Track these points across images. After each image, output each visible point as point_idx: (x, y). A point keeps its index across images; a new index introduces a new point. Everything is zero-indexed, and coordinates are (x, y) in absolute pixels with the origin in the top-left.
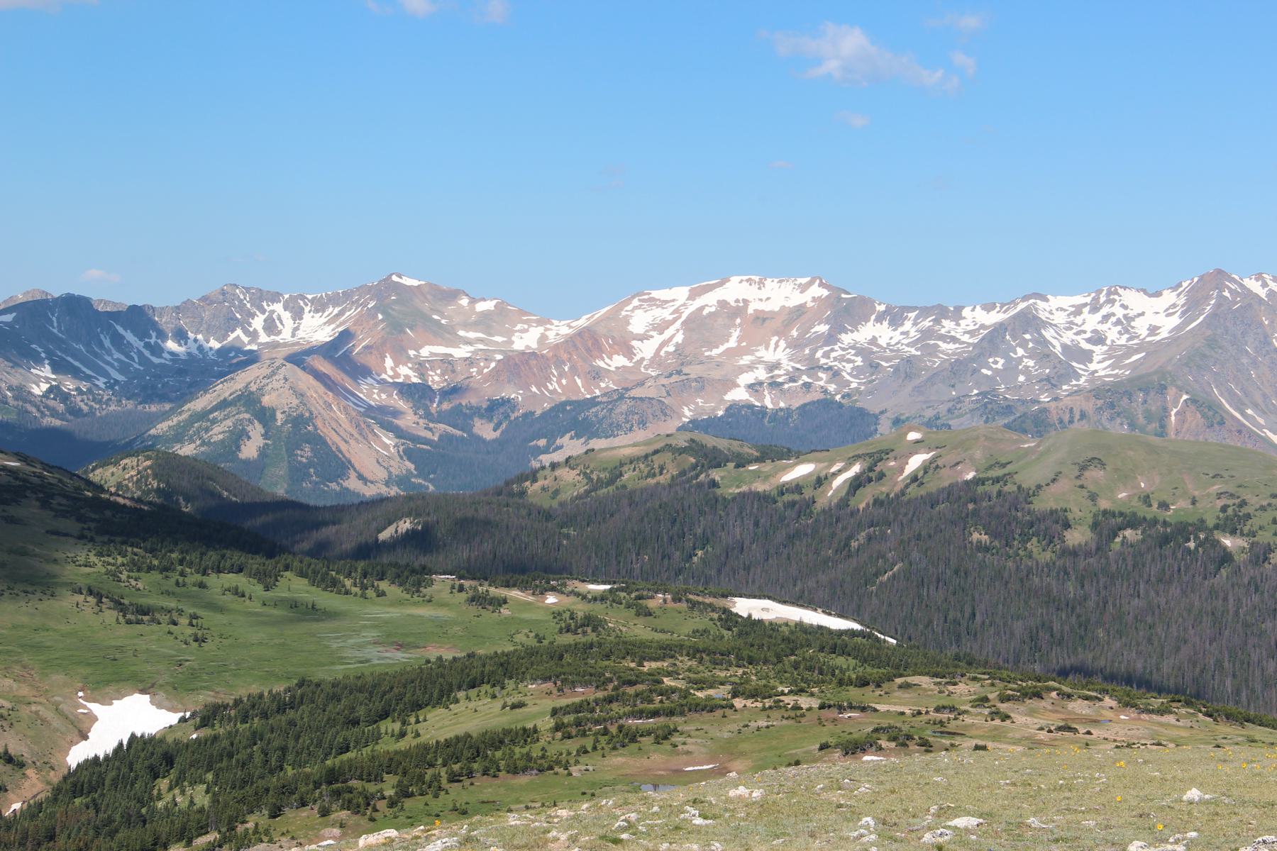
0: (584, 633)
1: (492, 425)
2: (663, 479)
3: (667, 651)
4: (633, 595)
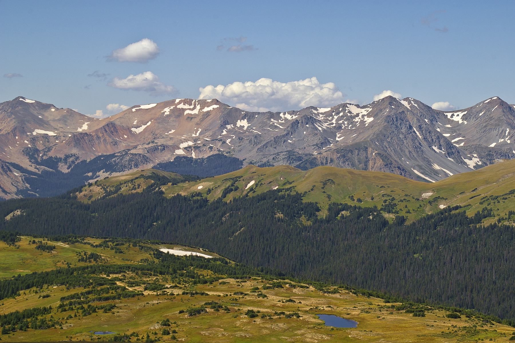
0: (90, 262)
1: (66, 166)
2: (140, 190)
3: (120, 269)
4: (114, 244)
